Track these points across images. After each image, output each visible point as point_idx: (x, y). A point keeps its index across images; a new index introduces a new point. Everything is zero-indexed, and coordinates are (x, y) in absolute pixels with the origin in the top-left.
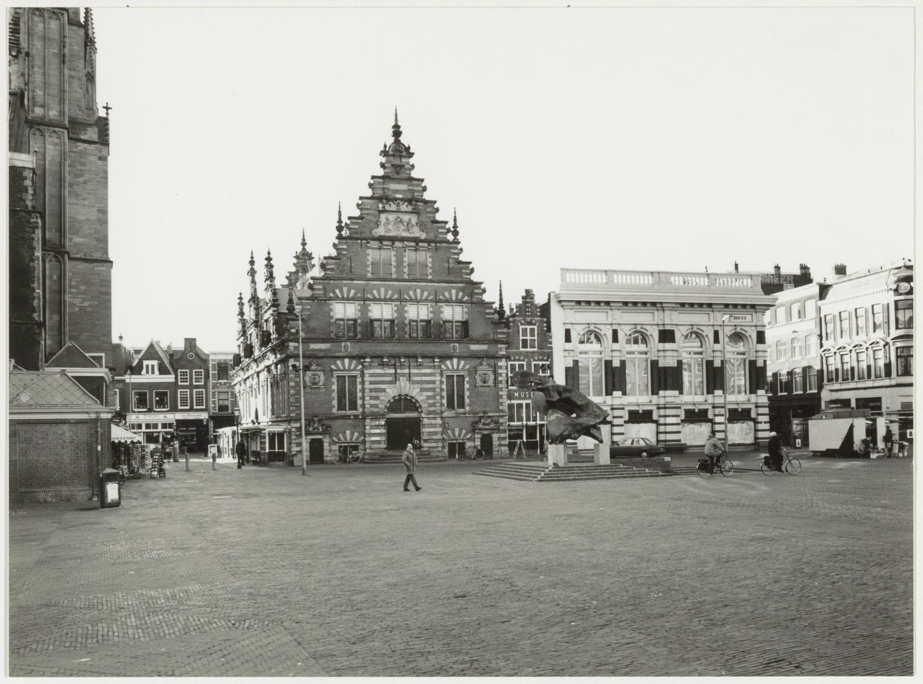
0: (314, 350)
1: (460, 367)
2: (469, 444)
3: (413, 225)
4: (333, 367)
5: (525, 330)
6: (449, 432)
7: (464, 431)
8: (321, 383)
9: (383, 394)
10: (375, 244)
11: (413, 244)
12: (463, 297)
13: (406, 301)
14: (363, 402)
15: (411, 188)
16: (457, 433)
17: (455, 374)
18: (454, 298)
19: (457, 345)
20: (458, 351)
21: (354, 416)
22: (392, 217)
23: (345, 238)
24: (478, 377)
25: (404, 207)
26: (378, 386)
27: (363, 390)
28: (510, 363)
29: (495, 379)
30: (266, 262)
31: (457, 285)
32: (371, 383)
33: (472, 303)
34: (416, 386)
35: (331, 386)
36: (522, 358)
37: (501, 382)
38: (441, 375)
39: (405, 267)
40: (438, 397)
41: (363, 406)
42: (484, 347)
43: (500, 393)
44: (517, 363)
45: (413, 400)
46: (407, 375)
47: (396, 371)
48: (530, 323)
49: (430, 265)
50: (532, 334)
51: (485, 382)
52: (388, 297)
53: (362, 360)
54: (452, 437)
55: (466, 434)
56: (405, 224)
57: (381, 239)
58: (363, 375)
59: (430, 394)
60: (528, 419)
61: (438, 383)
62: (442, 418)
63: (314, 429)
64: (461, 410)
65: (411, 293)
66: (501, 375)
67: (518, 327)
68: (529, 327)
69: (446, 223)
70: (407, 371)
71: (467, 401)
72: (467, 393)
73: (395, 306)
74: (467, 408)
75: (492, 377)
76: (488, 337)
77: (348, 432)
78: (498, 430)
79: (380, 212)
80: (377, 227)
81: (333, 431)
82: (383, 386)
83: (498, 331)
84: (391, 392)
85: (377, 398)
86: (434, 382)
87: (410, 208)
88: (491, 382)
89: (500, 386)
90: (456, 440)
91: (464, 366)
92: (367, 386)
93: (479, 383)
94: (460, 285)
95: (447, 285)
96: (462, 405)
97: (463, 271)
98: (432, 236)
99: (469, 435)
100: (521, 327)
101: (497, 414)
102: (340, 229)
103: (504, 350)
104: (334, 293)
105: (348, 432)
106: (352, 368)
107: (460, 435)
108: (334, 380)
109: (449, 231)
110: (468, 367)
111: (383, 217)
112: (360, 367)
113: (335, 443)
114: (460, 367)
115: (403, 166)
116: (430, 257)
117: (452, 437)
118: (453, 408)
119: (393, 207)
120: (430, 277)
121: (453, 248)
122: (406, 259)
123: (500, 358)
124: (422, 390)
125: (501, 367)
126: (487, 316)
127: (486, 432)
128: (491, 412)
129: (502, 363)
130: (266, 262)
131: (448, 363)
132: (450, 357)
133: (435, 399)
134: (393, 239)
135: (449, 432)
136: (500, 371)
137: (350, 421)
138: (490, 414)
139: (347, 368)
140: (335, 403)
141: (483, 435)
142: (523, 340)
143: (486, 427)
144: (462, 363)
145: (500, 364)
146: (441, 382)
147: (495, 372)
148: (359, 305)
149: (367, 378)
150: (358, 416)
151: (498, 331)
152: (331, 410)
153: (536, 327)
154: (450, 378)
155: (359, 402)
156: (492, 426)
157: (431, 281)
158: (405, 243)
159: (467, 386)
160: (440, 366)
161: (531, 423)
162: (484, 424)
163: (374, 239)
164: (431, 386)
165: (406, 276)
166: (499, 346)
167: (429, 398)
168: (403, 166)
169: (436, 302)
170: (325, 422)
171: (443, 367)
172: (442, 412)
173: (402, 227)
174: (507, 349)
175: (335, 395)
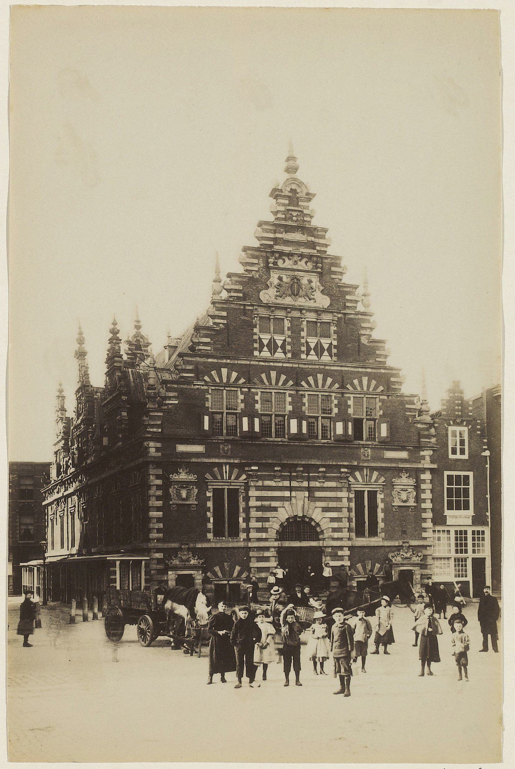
4: (208, 476)
9: (273, 514)
14: (248, 525)
16: (369, 567)
17: (367, 489)
25: (302, 265)
26: (266, 503)
27: (247, 510)
30: (111, 335)
32: (258, 499)
37: (424, 501)
38: (349, 490)
41: (247, 530)
43: (424, 515)
45: (313, 524)
53: (246, 469)
58: (247, 488)
59: (334, 515)
61: (345, 500)
69: (356, 287)
70: (305, 484)
71: (381, 525)
72: (380, 515)
73: (290, 395)
82: (274, 504)
85: (267, 520)
86: (339, 499)
87: (310, 266)
88: (412, 503)
92: (253, 503)
104: (211, 376)
110: (383, 479)
112: (244, 477)
119: (288, 263)
124: (325, 510)
130: (111, 335)
131: (357, 474)
144: (375, 474)
145: (423, 477)
146: (349, 500)
149: (253, 493)
154: (359, 495)
155: (243, 525)
159: (381, 506)
166: (422, 453)
167: (333, 520)
171: (351, 479)
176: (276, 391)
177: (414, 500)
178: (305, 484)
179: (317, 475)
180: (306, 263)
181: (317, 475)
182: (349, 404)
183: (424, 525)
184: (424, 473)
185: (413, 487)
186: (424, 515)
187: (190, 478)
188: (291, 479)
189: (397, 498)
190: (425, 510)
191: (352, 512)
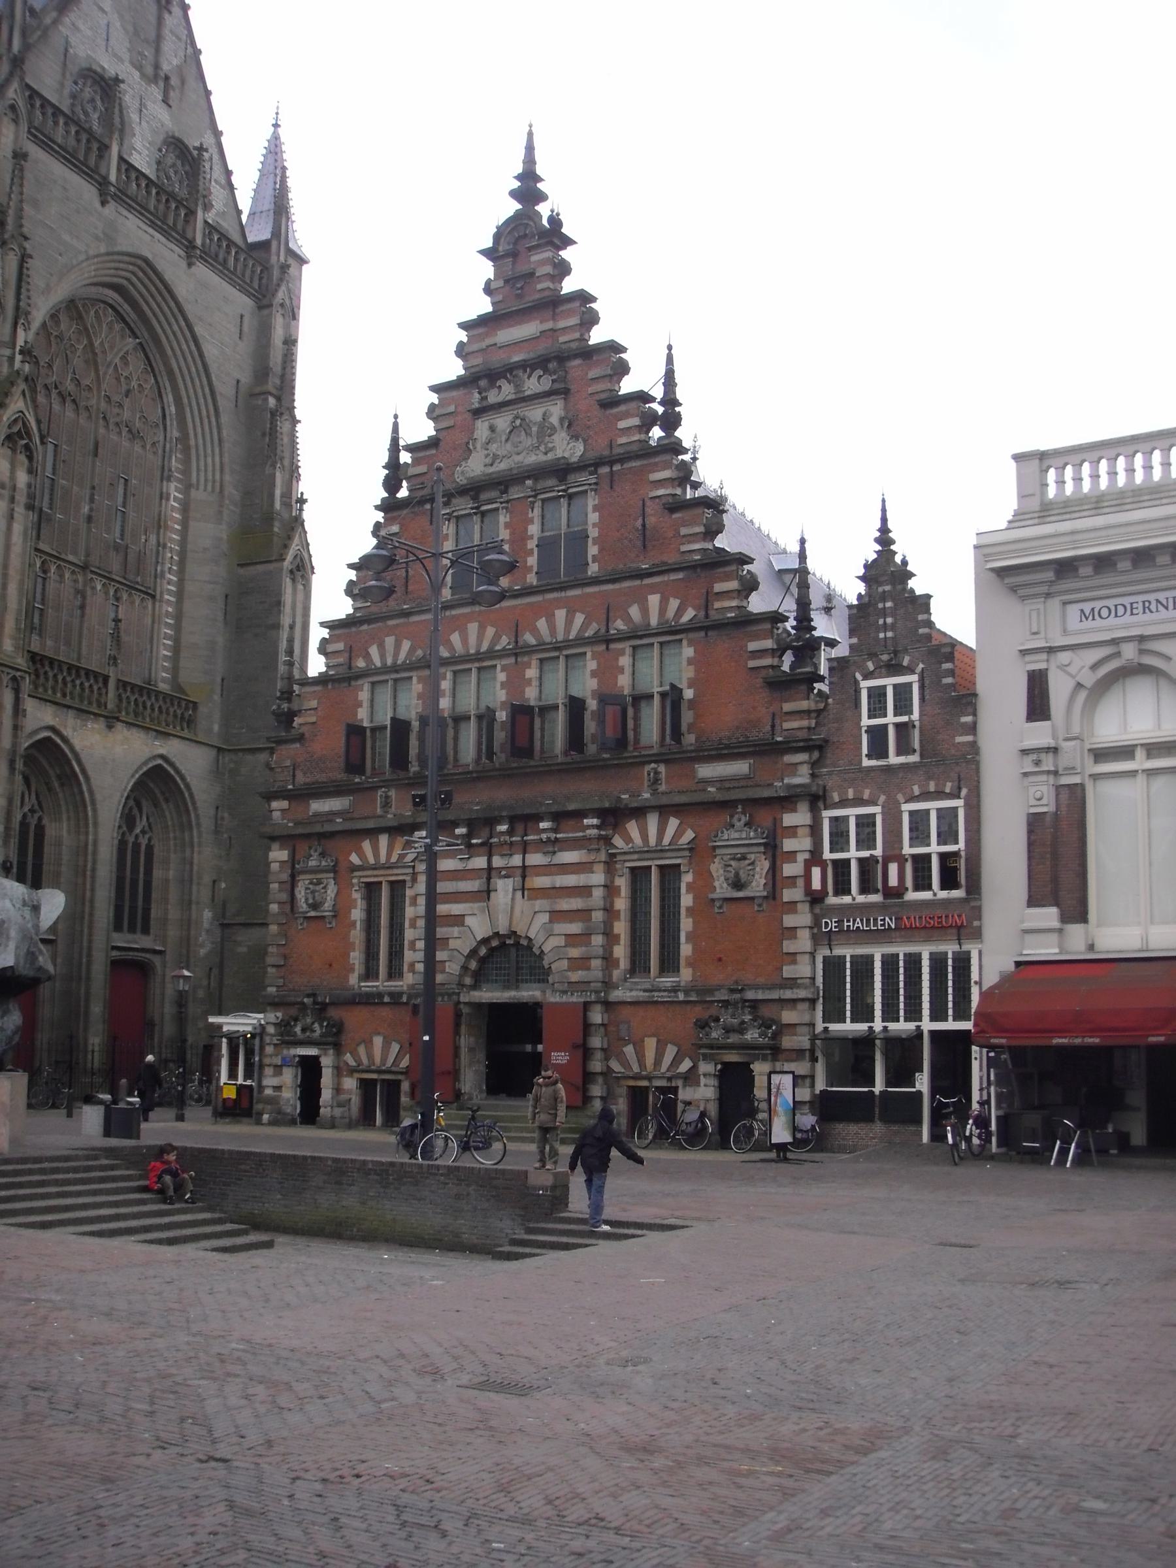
0: (316, 815)
1: (666, 840)
2: (684, 1094)
3: (553, 429)
4: (354, 859)
5: (877, 696)
6: (629, 1050)
7: (670, 1052)
8: (328, 905)
9: (455, 931)
10: (463, 505)
11: (551, 482)
12: (680, 611)
13: (530, 650)
15: (549, 325)
18: (654, 621)
19: (662, 768)
20: (662, 788)
21: (391, 994)
22: (503, 422)
23: (405, 503)
24: (716, 868)
25: (533, 384)
28: (827, 814)
29: (774, 870)
31: (665, 578)
33: (706, 629)
34: (539, 904)
35: (350, 912)
36: (866, 794)
38: (610, 865)
39: (531, 552)
40: (598, 940)
42: (740, 767)
43: (789, 921)
44: (852, 812)
46: (519, 872)
47: (489, 862)
48: (894, 668)
49: (593, 533)
50: (903, 706)
51: (738, 884)
52: (485, 647)
54: (636, 1068)
55: (676, 1061)
56: (534, 429)
57: (474, 490)
59: (575, 928)
60: (890, 1014)
62: (608, 1005)
63: (304, 1030)
64: (668, 981)
65: (542, 624)
66: (791, 856)
67: (856, 682)
68: (889, 682)
71: (686, 950)
72: (686, 924)
74: (686, 974)
75: (764, 865)
76: (754, 735)
77: (378, 1041)
78: (774, 1052)
79: (478, 413)
80: (466, 459)
81: (345, 1039)
83: (787, 707)
84: (478, 926)
86: (584, 891)
89: (788, 895)
90: (649, 1078)
91: (678, 834)
93: (722, 888)
94: (673, 576)
95: (637, 582)
96: (669, 963)
97: (684, 531)
98: (600, 447)
99: (686, 1065)
100: (865, 684)
101: (775, 995)
102: (391, 484)
103: (805, 770)
105: (378, 1041)
106: (394, 859)
107: (658, 1062)
108: (357, 896)
109: (651, 420)
110: (689, 835)
111: (481, 429)
113: (352, 1071)
114: (666, 840)
115: (532, 274)
116: (595, 508)
117: (636, 1068)
118: (647, 970)
119: (507, 391)
120: (593, 569)
121: (655, 468)
122: (534, 529)
123: (788, 801)
124: (557, 916)
125: (792, 831)
126: (752, 664)
127: (733, 1057)
128: (757, 987)
129: (799, 817)
132: (639, 813)
133: (588, 944)
134: (503, 483)
135: (629, 1050)
136: (789, 845)
137: (384, 1012)
138: (750, 995)
139: (383, 859)
140: (356, 957)
141: (727, 1066)
142: (871, 730)
143: (733, 1039)
145: (789, 820)
146: (610, 890)
147: (772, 848)
148: (420, 680)
150: (400, 994)
151: (787, 707)
152: (347, 978)
153: (913, 678)
154: (639, 876)
156: (752, 1035)
157: (595, 581)
158: (529, 482)
159: (686, 900)
160: (607, 841)
161: (903, 1027)
162: (728, 1030)
163: (463, 491)
164: (575, 903)
165: (532, 579)
167: (572, 940)
168: (532, 274)
169: (608, 641)
170: (333, 1013)
172: (608, 985)
173: (529, 442)
174: (814, 765)
175: (357, 935)
176: (477, 665)
177: (763, 881)
178: (517, 860)
179: (581, 834)
180: (540, 377)
181: (581, 834)
182: (620, 664)
183: (788, 946)
184: (794, 810)
185: (762, 849)
186: (789, 921)
187: (324, 863)
188: (489, 849)
189: (722, 879)
190: (792, 906)
191: (618, 918)
